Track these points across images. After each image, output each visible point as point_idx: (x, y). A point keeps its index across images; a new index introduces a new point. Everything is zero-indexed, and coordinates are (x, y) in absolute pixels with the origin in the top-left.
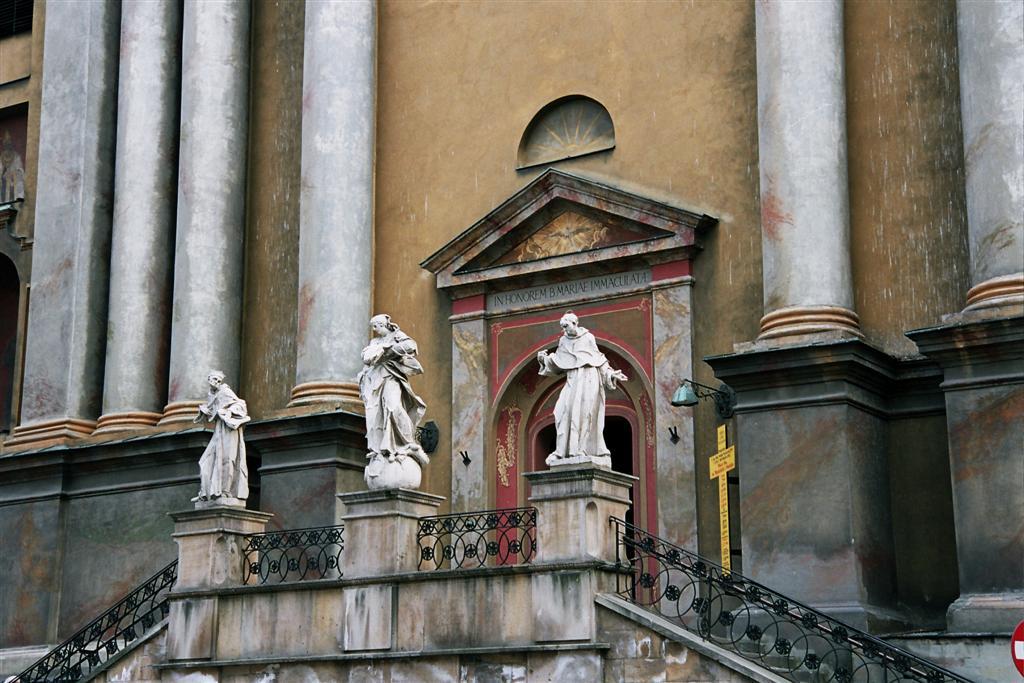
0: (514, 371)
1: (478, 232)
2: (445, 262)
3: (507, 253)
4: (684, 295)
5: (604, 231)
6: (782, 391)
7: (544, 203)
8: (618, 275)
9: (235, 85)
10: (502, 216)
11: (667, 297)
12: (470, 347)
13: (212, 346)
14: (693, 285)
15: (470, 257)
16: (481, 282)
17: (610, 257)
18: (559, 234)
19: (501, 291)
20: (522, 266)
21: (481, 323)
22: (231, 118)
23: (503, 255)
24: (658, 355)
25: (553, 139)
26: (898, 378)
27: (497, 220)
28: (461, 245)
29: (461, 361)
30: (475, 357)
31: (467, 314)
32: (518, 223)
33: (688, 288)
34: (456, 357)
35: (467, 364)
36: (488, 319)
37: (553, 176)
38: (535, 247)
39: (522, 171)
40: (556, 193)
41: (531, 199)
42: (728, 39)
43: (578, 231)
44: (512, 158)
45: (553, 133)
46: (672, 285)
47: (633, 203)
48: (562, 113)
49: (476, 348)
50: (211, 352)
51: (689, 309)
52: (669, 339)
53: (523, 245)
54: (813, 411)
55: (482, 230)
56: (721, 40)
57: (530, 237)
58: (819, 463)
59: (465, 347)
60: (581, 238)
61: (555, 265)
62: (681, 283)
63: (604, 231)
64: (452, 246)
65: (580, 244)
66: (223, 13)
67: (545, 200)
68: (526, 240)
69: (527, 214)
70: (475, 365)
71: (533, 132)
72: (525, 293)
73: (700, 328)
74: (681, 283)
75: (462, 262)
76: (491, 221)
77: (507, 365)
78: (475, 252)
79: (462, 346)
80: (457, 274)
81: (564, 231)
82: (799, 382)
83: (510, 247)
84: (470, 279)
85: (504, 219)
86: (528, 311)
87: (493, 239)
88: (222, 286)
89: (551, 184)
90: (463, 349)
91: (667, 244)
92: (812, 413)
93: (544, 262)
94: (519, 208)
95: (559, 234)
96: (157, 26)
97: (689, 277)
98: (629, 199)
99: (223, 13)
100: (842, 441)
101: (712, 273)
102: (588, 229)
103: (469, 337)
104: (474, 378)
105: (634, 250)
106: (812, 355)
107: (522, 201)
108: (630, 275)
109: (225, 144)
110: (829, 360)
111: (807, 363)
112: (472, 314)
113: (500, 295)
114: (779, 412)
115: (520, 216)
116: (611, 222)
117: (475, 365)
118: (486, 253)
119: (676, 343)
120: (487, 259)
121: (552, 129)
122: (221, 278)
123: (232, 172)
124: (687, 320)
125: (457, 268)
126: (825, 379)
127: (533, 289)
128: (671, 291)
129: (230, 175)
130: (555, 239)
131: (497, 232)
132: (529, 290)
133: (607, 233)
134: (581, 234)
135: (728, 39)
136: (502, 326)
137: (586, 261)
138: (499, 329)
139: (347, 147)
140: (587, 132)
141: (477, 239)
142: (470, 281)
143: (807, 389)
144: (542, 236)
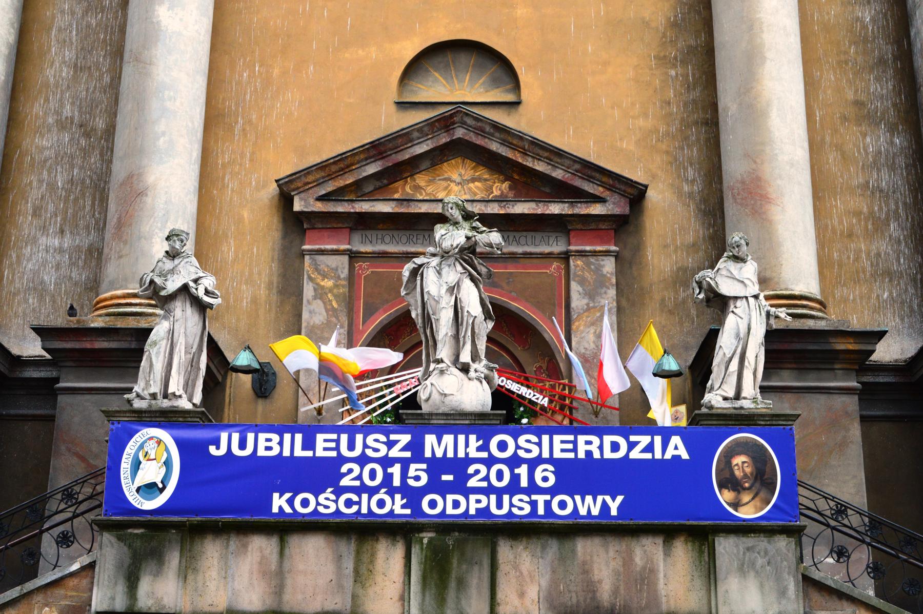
0: (381, 318)
2: (310, 183)
3: (380, 188)
4: (609, 266)
5: (506, 185)
6: (786, 373)
7: (444, 141)
11: (588, 264)
12: (328, 283)
14: (617, 256)
15: (340, 183)
17: (526, 212)
18: (449, 179)
19: (370, 229)
21: (346, 259)
23: (376, 189)
24: (577, 324)
25: (436, 80)
26: (917, 377)
28: (334, 168)
29: (315, 298)
30: (335, 296)
31: (329, 247)
33: (613, 259)
34: (308, 291)
35: (324, 303)
36: (354, 256)
38: (417, 188)
39: (402, 105)
40: (459, 133)
42: (653, 25)
43: (473, 180)
44: (392, 92)
45: (437, 75)
46: (595, 253)
49: (336, 286)
51: (614, 281)
52: (589, 309)
53: (401, 182)
54: (823, 398)
56: (646, 24)
57: (412, 176)
58: (831, 452)
59: (322, 284)
62: (607, 253)
63: (506, 185)
64: (322, 166)
65: (475, 194)
68: (407, 178)
69: (419, 149)
70: (335, 306)
71: (415, 67)
72: (404, 235)
73: (624, 303)
74: (607, 253)
75: (330, 187)
76: (376, 149)
77: (370, 311)
78: (349, 180)
79: (319, 281)
80: (320, 199)
81: (455, 177)
82: (808, 366)
83: (385, 181)
84: (341, 208)
87: (372, 169)
89: (454, 123)
90: (318, 284)
91: (597, 209)
92: (821, 400)
94: (411, 141)
95: (449, 179)
97: (613, 248)
98: (555, 154)
100: (855, 431)
101: (638, 249)
102: (486, 180)
103: (327, 269)
104: (334, 319)
105: (555, 209)
106: (832, 340)
110: (851, 347)
111: (827, 347)
112: (335, 247)
113: (369, 233)
114: (784, 395)
117: (335, 306)
118: (358, 184)
119: (598, 314)
120: (357, 190)
124: (612, 292)
125: (324, 192)
126: (837, 366)
128: (592, 260)
130: (444, 184)
132: (408, 233)
133: (511, 188)
134: (477, 183)
135: (653, 25)
136: (369, 267)
138: (365, 269)
139: (197, 31)
140: (481, 81)
143: (813, 375)
144: (427, 178)
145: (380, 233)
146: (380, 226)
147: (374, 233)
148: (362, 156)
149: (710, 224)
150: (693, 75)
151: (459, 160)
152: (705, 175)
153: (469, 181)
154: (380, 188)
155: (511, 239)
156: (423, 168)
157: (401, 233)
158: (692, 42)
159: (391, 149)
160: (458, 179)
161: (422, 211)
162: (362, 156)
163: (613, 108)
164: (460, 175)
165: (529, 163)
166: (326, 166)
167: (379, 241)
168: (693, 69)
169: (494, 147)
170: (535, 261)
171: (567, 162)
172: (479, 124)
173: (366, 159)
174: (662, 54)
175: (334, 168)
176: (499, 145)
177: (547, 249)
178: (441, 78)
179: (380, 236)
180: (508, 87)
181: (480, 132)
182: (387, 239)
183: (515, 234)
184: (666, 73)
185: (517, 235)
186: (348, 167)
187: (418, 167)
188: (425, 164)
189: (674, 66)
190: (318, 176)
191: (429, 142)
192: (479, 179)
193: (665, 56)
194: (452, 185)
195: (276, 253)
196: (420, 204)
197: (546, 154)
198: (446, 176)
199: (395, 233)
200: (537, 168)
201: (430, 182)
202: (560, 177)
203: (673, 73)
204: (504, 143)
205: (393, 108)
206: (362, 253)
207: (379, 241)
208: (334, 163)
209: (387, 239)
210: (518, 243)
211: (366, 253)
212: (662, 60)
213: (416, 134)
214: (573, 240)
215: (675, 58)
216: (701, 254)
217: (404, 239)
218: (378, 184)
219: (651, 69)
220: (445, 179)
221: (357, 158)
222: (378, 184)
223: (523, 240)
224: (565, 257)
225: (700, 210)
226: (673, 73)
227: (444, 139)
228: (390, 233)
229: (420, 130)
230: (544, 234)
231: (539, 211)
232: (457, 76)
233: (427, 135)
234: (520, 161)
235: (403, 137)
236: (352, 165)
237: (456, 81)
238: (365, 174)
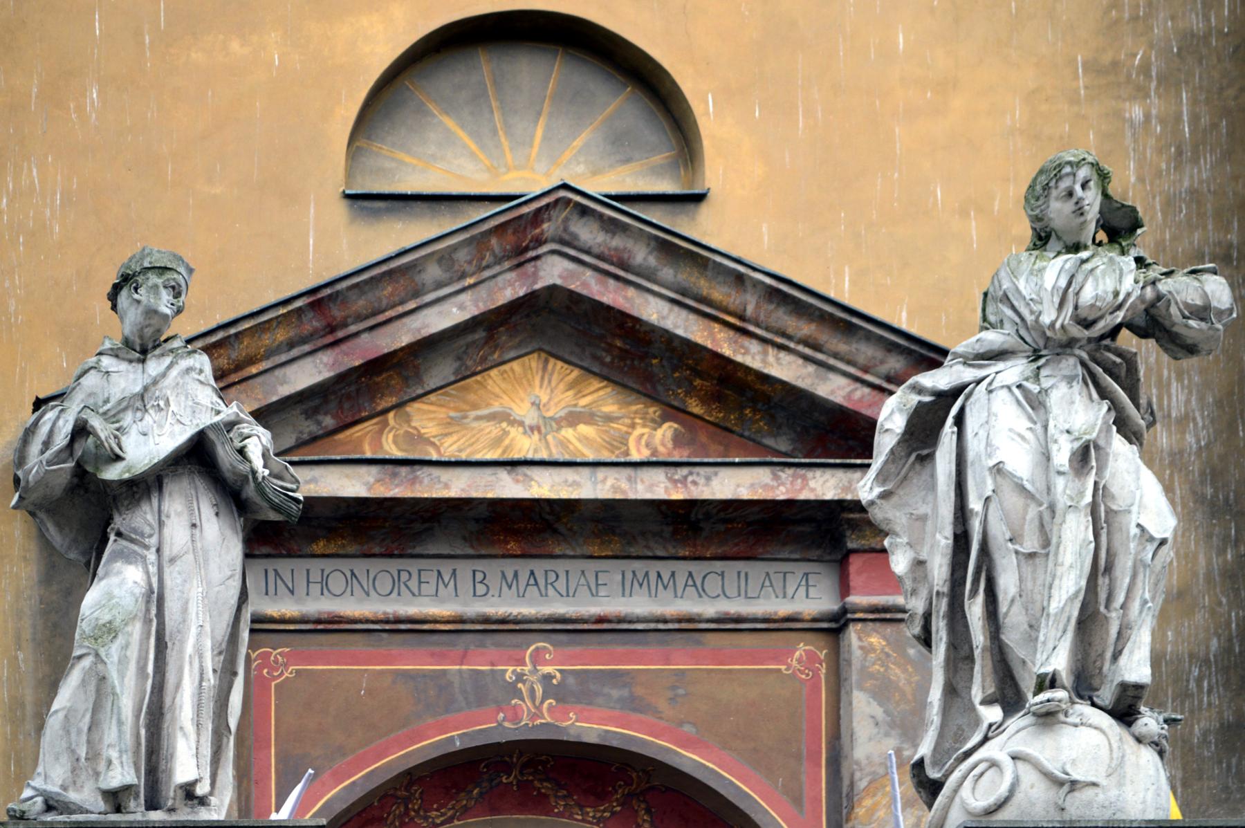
1: (267, 340)
5: (667, 431)
8: (718, 565)
17: (745, 494)
19: (290, 555)
20: (423, 472)
32: (405, 340)
41: (463, 276)
45: (449, 122)
47: (842, 347)
53: (369, 426)
55: (281, 335)
60: (584, 439)
67: (508, 288)
72: (382, 570)
81: (523, 410)
83: (329, 422)
85: (360, 318)
108: (756, 570)
115: (631, 292)
116: (697, 409)
121: (449, 108)
127: (413, 565)
131: (326, 357)
132: (393, 565)
140: (578, 143)
141: (251, 361)
145: (316, 565)
146: (319, 547)
147: (300, 565)
149: (1226, 539)
150: (1195, 119)
151: (533, 361)
152: (1219, 404)
153: (560, 423)
154: (314, 439)
155: (681, 579)
156: (432, 383)
157: (376, 565)
158: (1195, 23)
160: (531, 417)
161: (453, 493)
162: (281, 335)
163: (964, 213)
164: (536, 405)
165: (753, 356)
167: (315, 589)
168: (1194, 102)
169: (654, 311)
170: (748, 641)
171: (865, 351)
172: (617, 242)
174: (1107, 58)
177: (783, 608)
178: (461, 134)
179: (316, 576)
180: (658, 159)
181: (618, 268)
182: (337, 582)
183: (694, 567)
184: (1118, 115)
185: (698, 568)
188: (440, 371)
189: (1141, 93)
191: (465, 298)
192: (588, 417)
193: (1115, 64)
194: (515, 432)
195: (27, 623)
196: (445, 474)
197: (806, 329)
199: (360, 566)
200: (776, 371)
201: (452, 424)
202: (838, 398)
203: (1137, 112)
204: (683, 299)
205: (341, 209)
206: (272, 620)
207: (315, 589)
209: (337, 582)
210: (702, 592)
211: (283, 621)
212: (1106, 73)
213: (433, 272)
214: (855, 580)
215: (1145, 69)
216: (1200, 617)
217: (385, 583)
218: (309, 428)
219: (1074, 100)
220: (493, 417)
222: (309, 428)
223: (713, 584)
224: (834, 627)
225: (1200, 499)
226: (1137, 112)
228: (345, 565)
229: (445, 259)
230: (773, 567)
231: (781, 494)
232: (508, 128)
234: (727, 351)
235: (395, 278)
237: (505, 143)
238: (285, 390)
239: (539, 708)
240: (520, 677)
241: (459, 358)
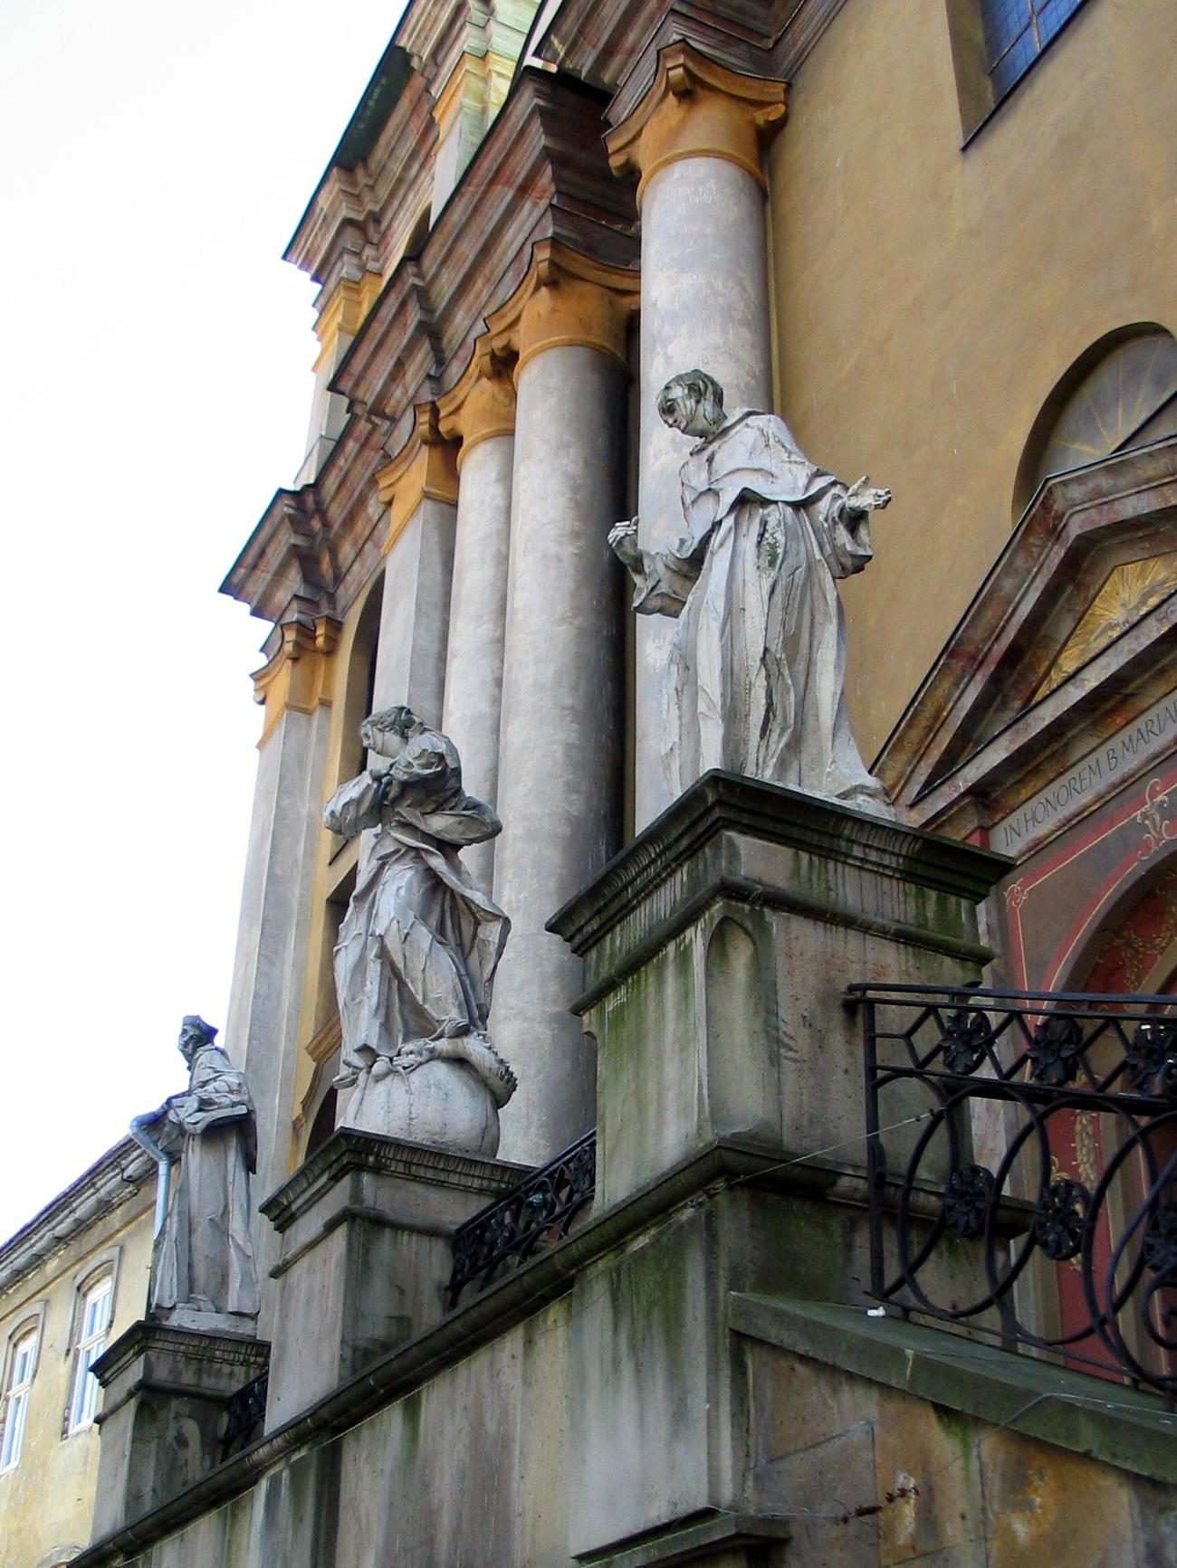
2: (894, 787)
9: (578, 656)
10: (978, 634)
13: (535, 1118)
15: (936, 754)
16: (963, 795)
22: (571, 708)
27: (970, 648)
28: (914, 735)
37: (1058, 493)
40: (1075, 529)
45: (1077, 446)
48: (1087, 392)
50: (533, 1130)
61: (1093, 678)
66: (554, 549)
78: (945, 739)
86: (1077, 823)
88: (555, 1002)
93: (1069, 688)
94: (1009, 603)
96: (485, 626)
99: (554, 549)
107: (1008, 584)
109: (558, 751)
122: (554, 987)
123: (574, 797)
129: (571, 803)
136: (1024, 885)
137: (1155, 635)
142: (941, 805)
146: (1024, 794)
148: (946, 685)
156: (1064, 637)
159: (984, 641)
166: (900, 740)
173: (957, 685)
175: (914, 735)
176: (1134, 499)
186: (936, 718)
187: (1049, 638)
190: (899, 765)
198: (1104, 623)
208: (909, 726)
221: (940, 692)
227: (1057, 554)
233: (1029, 571)
236: (941, 709)
239: (1160, 833)
240: (1145, 816)
241: (1070, 611)
